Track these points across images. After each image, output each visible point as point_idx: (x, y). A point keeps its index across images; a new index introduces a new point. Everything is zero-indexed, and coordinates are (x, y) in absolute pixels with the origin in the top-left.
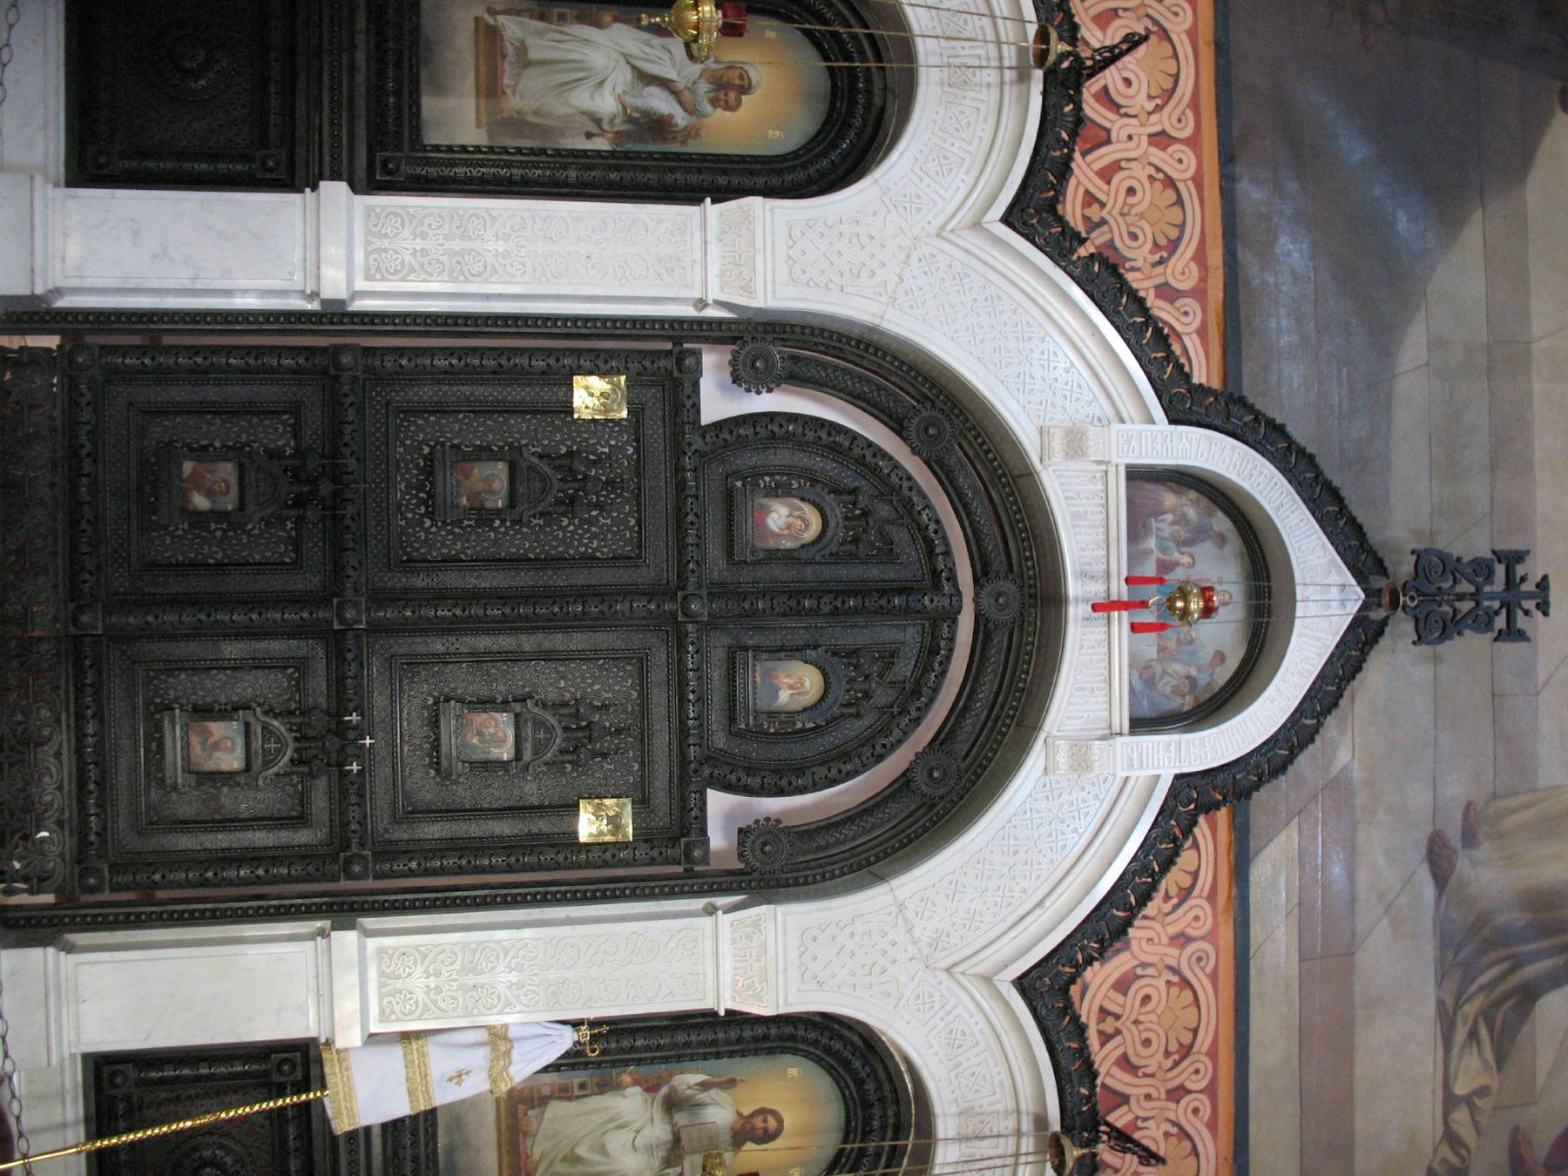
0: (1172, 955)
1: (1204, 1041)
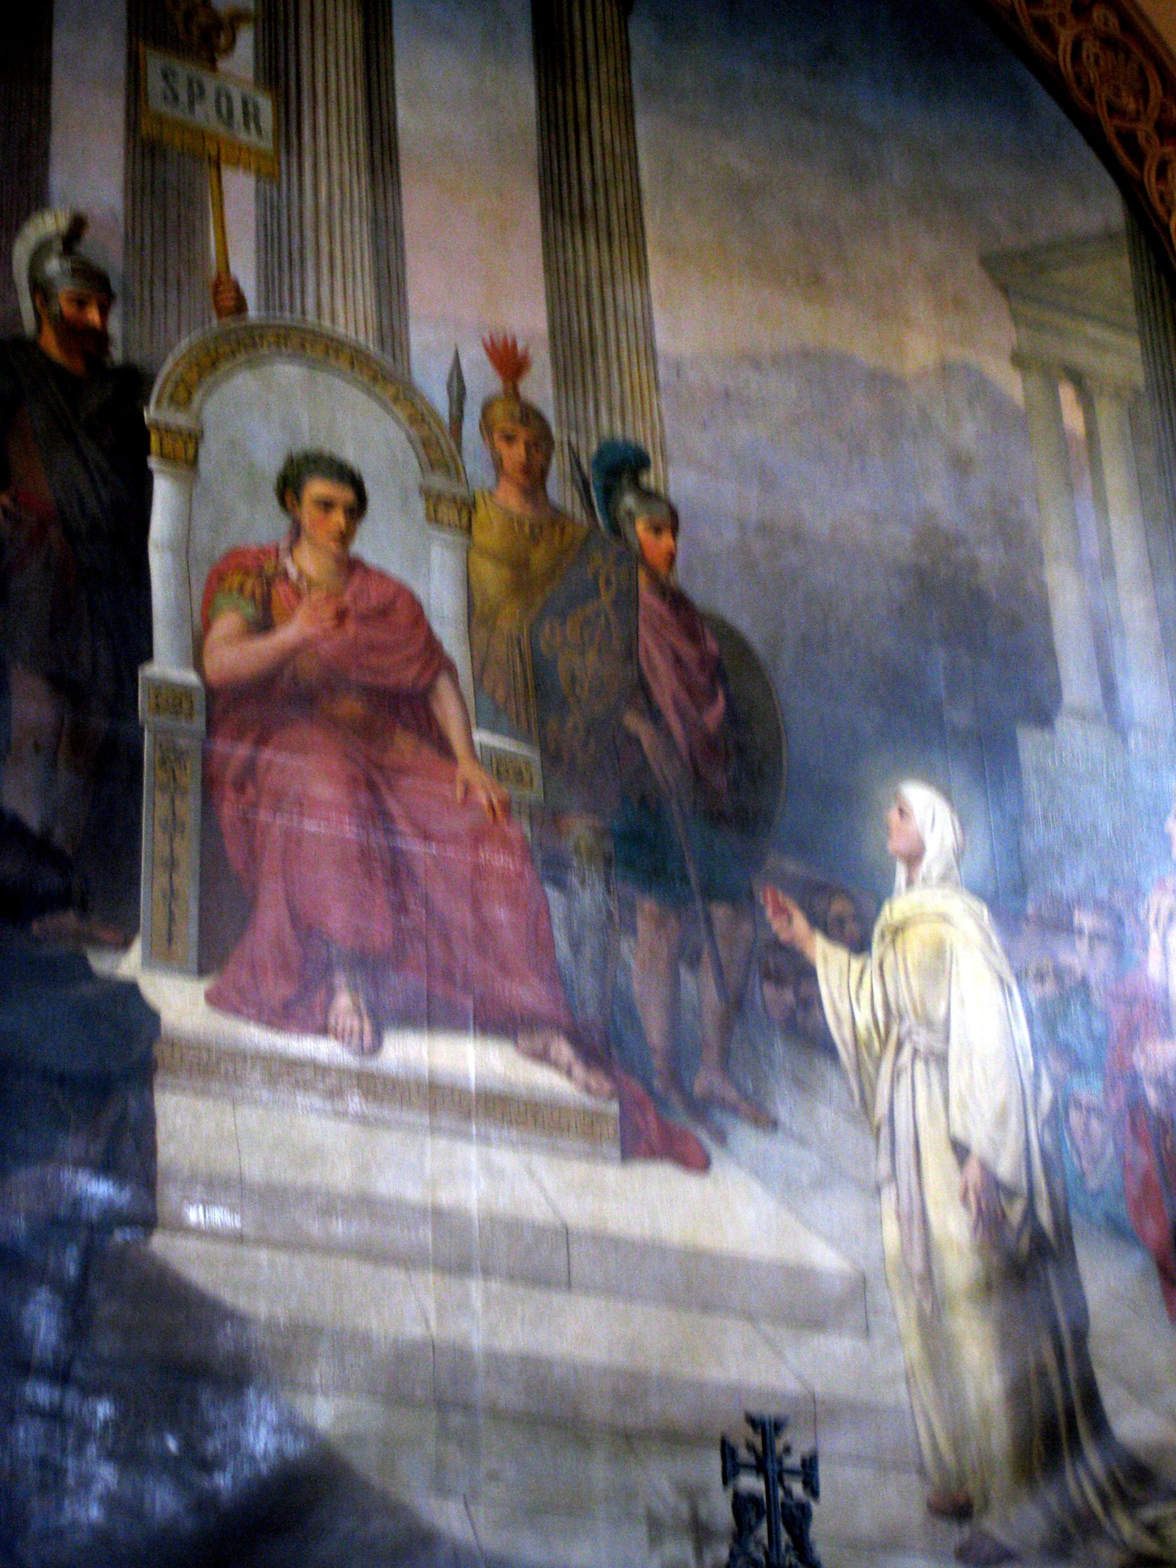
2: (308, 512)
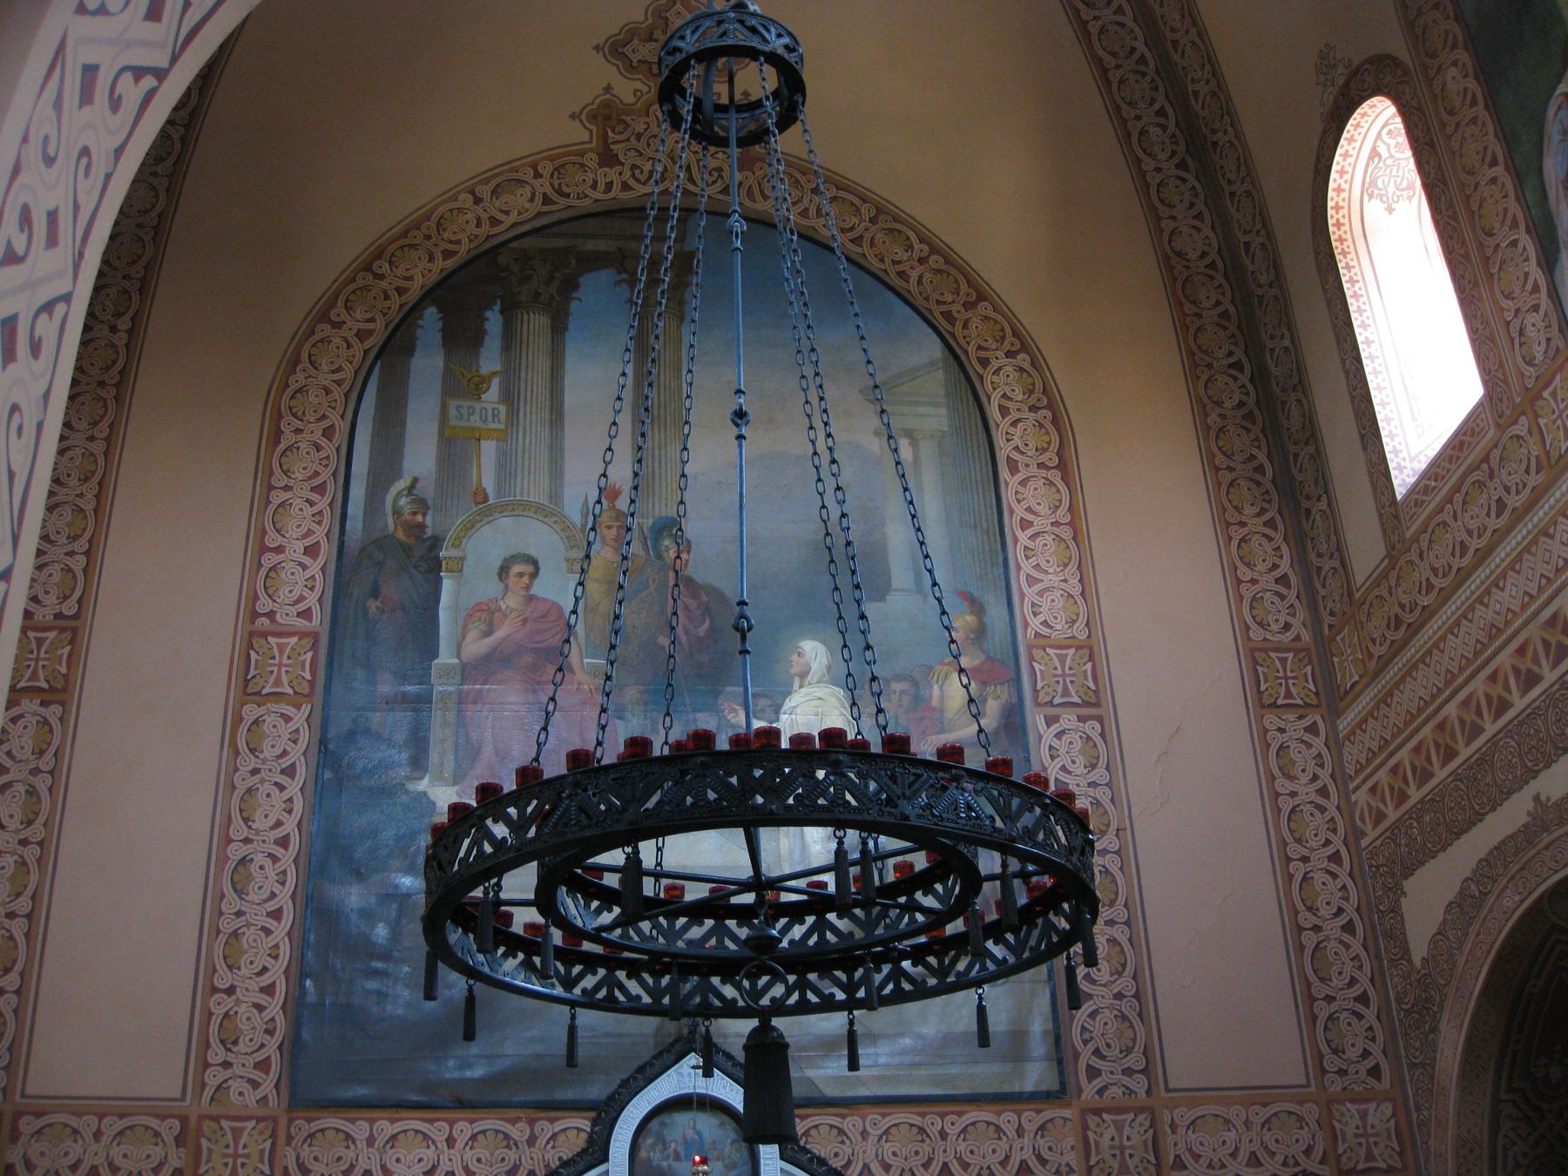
0: (872, 1140)
1: (917, 1120)
2: (512, 580)
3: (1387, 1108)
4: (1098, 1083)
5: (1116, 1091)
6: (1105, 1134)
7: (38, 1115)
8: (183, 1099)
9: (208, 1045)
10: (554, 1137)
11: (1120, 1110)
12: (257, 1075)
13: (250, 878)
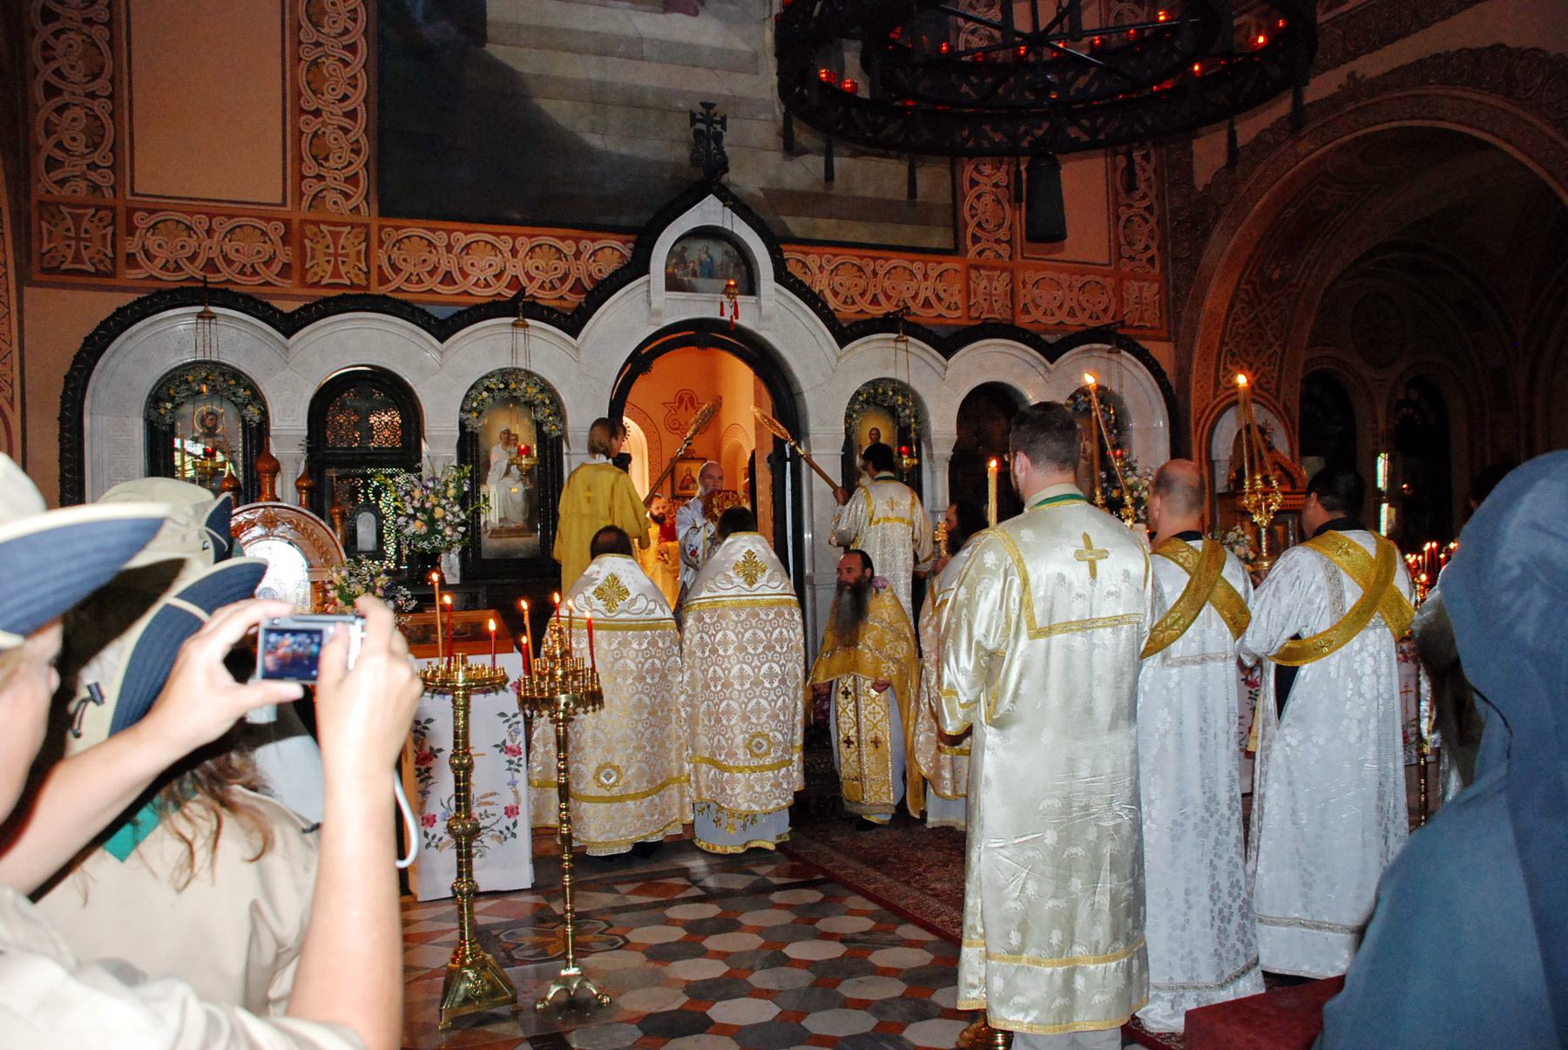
0: (826, 273)
1: (857, 261)
3: (1156, 286)
4: (979, 247)
5: (988, 253)
6: (981, 283)
7: (151, 212)
8: (284, 204)
9: (302, 160)
10: (594, 253)
11: (992, 268)
12: (348, 189)
13: (324, 12)
